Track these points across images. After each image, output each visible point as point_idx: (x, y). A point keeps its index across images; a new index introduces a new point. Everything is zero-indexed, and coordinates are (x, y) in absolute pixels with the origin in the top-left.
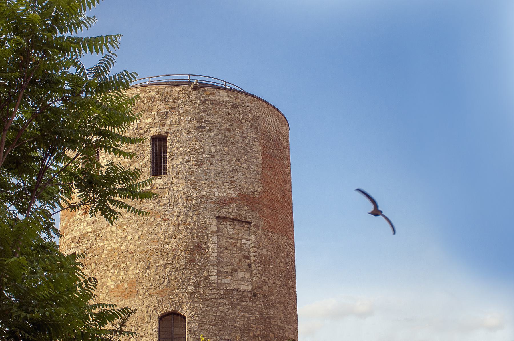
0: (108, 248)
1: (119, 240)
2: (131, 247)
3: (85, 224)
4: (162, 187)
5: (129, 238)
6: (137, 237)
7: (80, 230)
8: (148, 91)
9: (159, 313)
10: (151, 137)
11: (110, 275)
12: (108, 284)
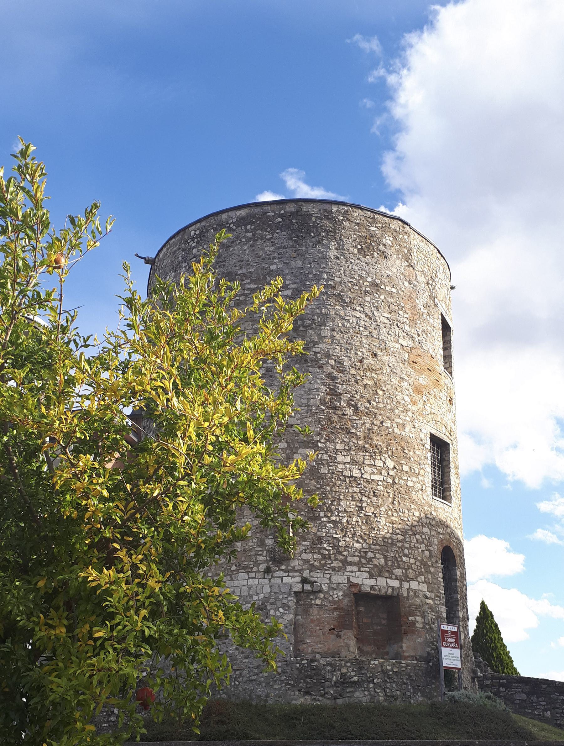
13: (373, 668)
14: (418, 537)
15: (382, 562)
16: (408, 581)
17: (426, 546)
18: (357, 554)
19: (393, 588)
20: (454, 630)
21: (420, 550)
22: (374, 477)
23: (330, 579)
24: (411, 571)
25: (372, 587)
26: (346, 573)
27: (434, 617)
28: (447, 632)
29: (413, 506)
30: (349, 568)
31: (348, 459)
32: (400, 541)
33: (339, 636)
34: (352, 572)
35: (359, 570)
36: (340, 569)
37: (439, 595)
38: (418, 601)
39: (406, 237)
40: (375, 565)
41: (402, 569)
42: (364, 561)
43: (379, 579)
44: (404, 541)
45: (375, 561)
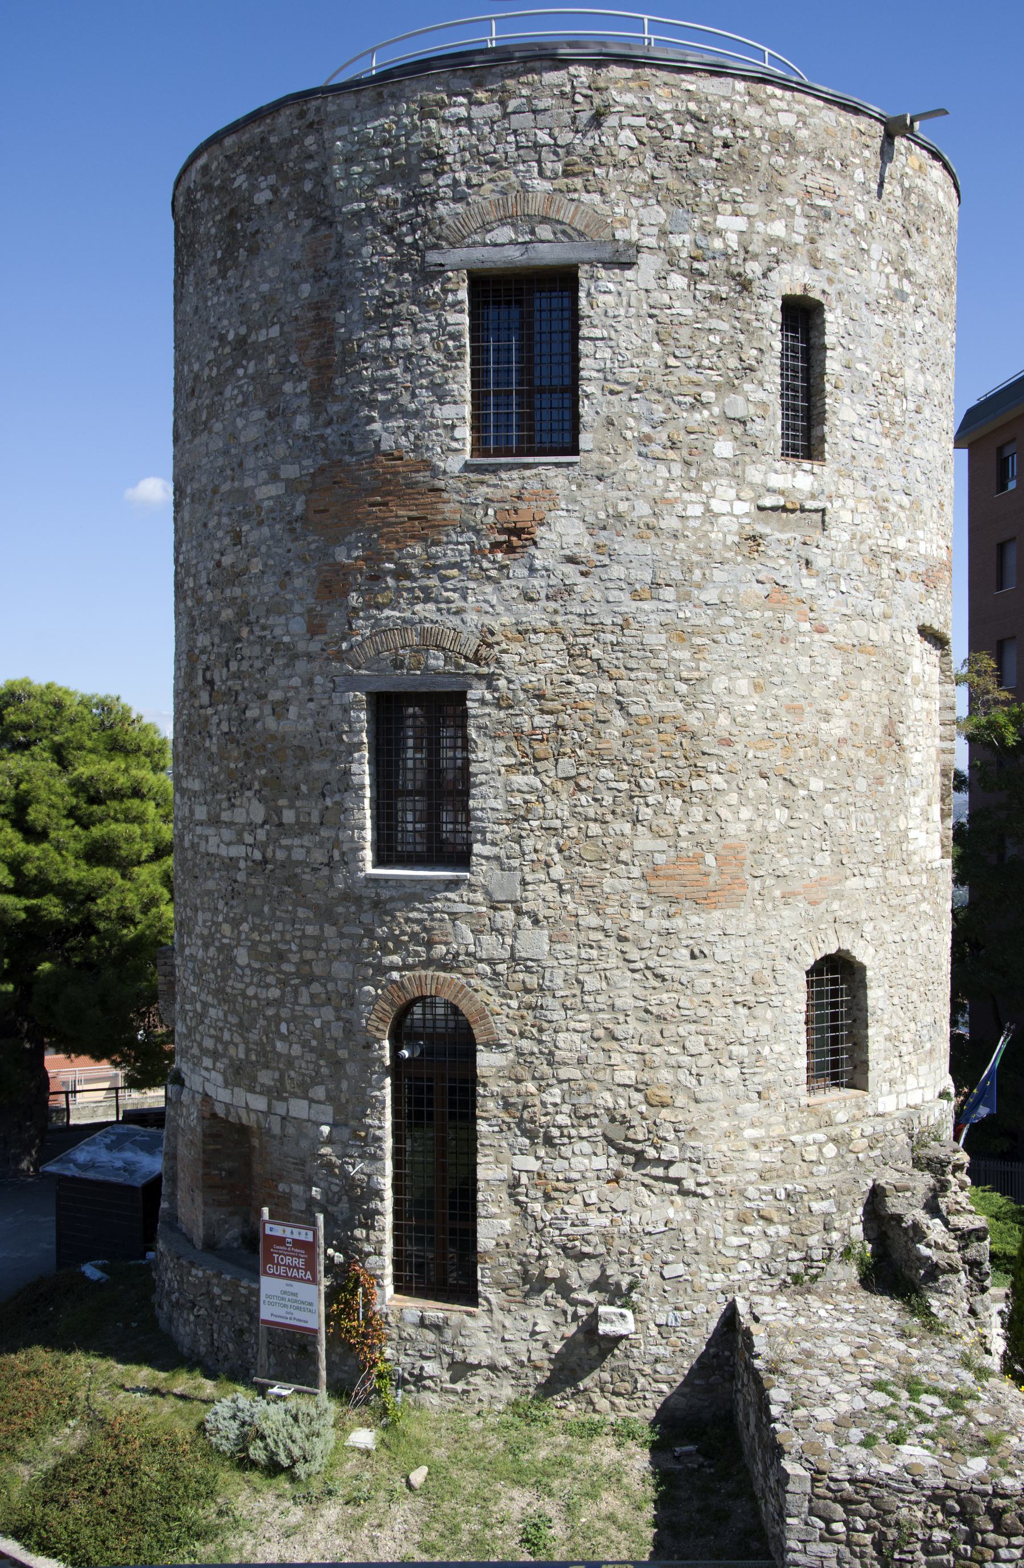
2: (723, 720)
5: (719, 684)
8: (774, 103)
11: (645, 813)
12: (640, 845)
14: (316, 988)
16: (286, 1100)
17: (337, 1009)
20: (303, 1238)
21: (318, 1023)
27: (335, 1189)
28: (281, 1241)
29: (302, 913)
41: (274, 1069)
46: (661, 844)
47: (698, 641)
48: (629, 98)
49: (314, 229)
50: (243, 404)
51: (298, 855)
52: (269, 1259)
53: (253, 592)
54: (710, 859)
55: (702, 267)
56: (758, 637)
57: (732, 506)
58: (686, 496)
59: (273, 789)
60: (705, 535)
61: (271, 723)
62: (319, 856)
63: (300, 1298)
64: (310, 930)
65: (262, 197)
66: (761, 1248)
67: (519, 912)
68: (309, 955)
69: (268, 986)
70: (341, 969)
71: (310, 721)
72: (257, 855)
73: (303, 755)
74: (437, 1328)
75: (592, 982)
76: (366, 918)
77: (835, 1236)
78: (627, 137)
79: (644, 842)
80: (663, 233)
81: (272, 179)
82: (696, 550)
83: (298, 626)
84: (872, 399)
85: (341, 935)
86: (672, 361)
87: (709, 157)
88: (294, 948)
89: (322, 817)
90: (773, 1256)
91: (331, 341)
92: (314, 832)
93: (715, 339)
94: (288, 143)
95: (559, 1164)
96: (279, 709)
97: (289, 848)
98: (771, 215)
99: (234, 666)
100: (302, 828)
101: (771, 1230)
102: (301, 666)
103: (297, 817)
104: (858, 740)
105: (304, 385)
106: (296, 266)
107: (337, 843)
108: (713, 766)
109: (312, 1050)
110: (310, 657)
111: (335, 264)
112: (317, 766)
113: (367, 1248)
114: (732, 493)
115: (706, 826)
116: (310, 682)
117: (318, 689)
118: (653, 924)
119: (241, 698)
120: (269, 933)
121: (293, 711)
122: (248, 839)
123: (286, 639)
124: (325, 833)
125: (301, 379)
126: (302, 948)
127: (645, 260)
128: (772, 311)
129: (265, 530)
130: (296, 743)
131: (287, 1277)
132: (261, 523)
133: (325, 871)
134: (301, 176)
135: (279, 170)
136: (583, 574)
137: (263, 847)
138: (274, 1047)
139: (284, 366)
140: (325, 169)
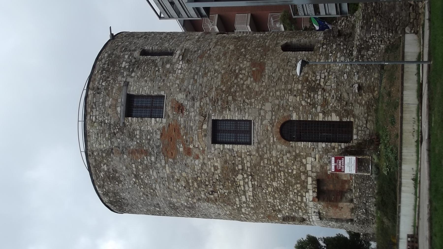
0: (219, 84)
1: (216, 74)
2: (224, 66)
3: (192, 110)
4: (183, 51)
5: (217, 67)
6: (218, 63)
7: (195, 116)
9: (281, 51)
10: (140, 55)
11: (242, 82)
13: (358, 202)
14: (279, 161)
15: (298, 186)
16: (307, 171)
17: (283, 155)
18: (296, 197)
19: (312, 181)
20: (334, 160)
21: (288, 161)
22: (250, 186)
23: (311, 208)
24: (301, 169)
25: (314, 192)
26: (308, 202)
28: (335, 166)
29: (262, 164)
30: (305, 200)
31: (243, 197)
32: (284, 174)
33: (342, 208)
34: (306, 200)
35: (305, 196)
36: (305, 204)
37: (312, 149)
38: (318, 166)
39: (95, 154)
40: (301, 189)
42: (299, 194)
43: (308, 188)
44: (284, 171)
45: (299, 189)
46: (249, 78)
47: (207, 71)
48: (96, 83)
49: (113, 154)
50: (149, 176)
51: (249, 165)
52: (340, 170)
53: (190, 176)
54: (254, 69)
55: (131, 69)
56: (208, 60)
57: (181, 65)
58: (176, 73)
59: (235, 172)
60: (185, 69)
61: (219, 171)
62: (248, 158)
63: (349, 162)
64: (266, 162)
65: (105, 168)
66: (342, 59)
67: (261, 109)
68: (272, 162)
69: (281, 175)
70: (274, 153)
71: (218, 159)
72: (250, 177)
73: (226, 162)
74: (358, 131)
75: (278, 93)
76: (262, 146)
77: (341, 43)
78: (103, 84)
79: (248, 82)
80: (123, 77)
81: (102, 165)
82: (188, 71)
83: (197, 162)
84: (165, 42)
85: (266, 153)
86: (149, 75)
87: (110, 68)
88: (270, 167)
89: (239, 157)
90: (344, 56)
91: (136, 150)
92: (243, 160)
93: (146, 67)
94: (96, 160)
95: (320, 102)
96: (216, 168)
97: (248, 167)
98: (124, 57)
99: (207, 183)
100: (243, 164)
101: (338, 57)
102: (206, 162)
103: (240, 164)
104: (236, 43)
105: (145, 157)
106: (120, 159)
107: (245, 153)
108: (234, 68)
109: (294, 162)
110: (204, 159)
111: (121, 148)
112: (228, 158)
113: (340, 148)
114: (177, 64)
115: (247, 70)
116: (209, 159)
117: (211, 157)
118: (266, 81)
119: (214, 181)
120: (268, 174)
121: (216, 164)
122: (247, 180)
123: (200, 165)
124: (243, 157)
125: (144, 158)
126: (270, 165)
127: (127, 80)
128: (141, 57)
129: (176, 171)
130: (223, 163)
131: (344, 165)
132: (175, 172)
133: (252, 157)
134: (103, 157)
135: (101, 162)
136: (190, 93)
137: (248, 175)
138: (296, 174)
139: (141, 163)
140: (101, 150)
